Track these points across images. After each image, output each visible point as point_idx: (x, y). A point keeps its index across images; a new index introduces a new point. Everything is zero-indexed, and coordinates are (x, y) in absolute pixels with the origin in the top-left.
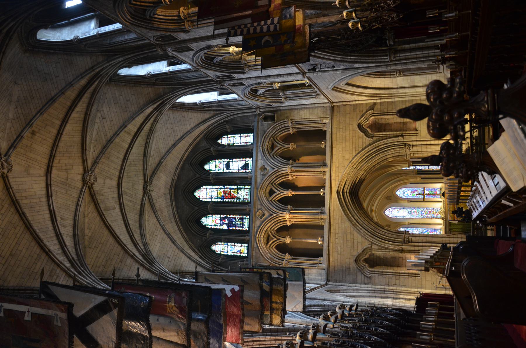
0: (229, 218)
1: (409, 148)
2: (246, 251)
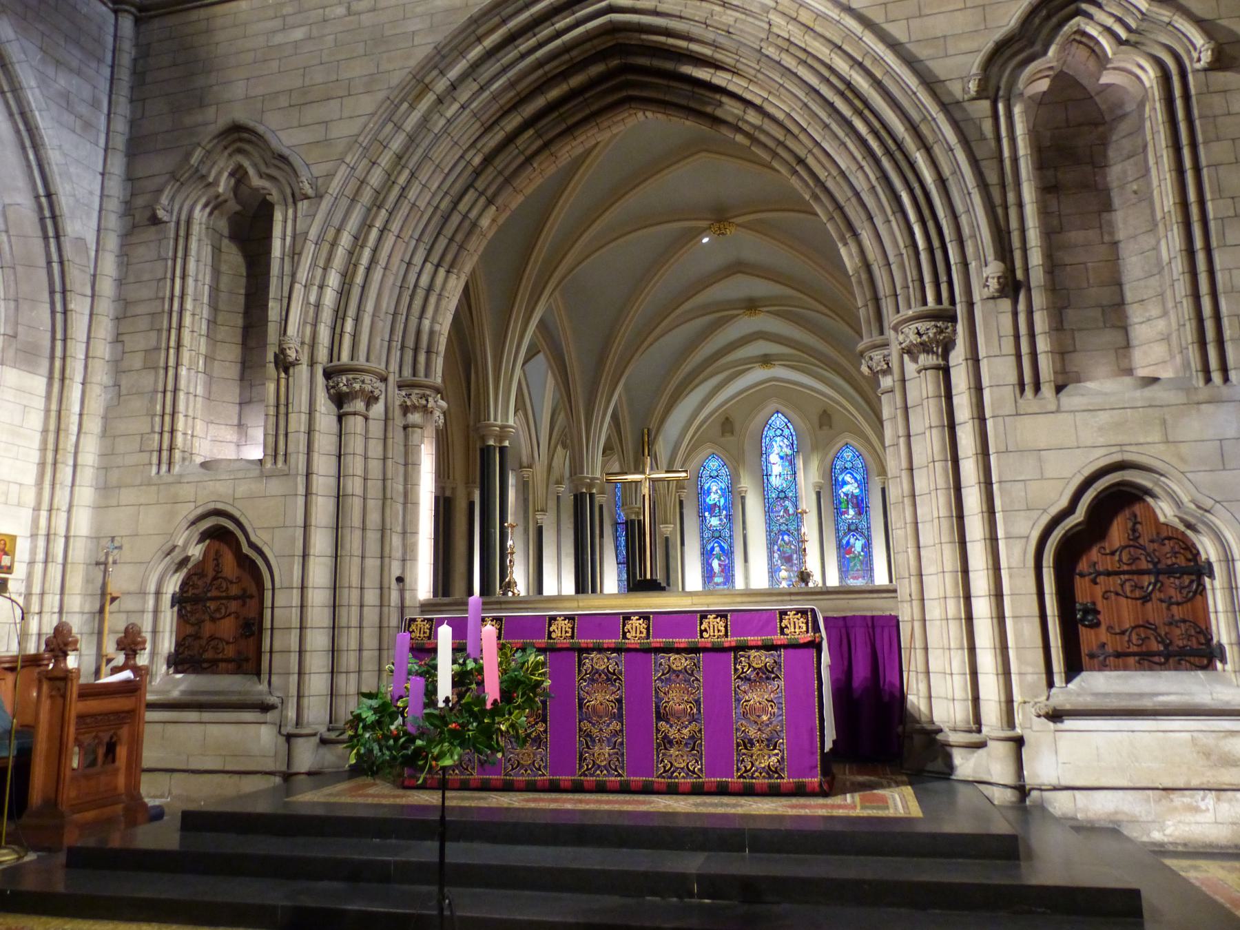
1: (925, 348)
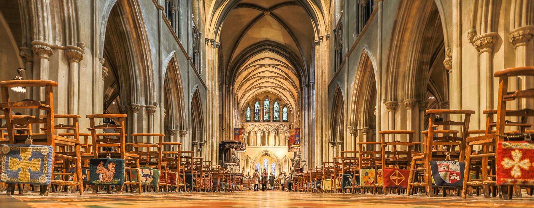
0: (258, 112)
2: (248, 120)
